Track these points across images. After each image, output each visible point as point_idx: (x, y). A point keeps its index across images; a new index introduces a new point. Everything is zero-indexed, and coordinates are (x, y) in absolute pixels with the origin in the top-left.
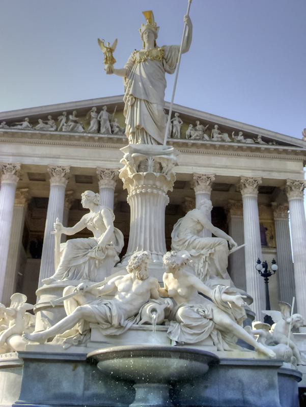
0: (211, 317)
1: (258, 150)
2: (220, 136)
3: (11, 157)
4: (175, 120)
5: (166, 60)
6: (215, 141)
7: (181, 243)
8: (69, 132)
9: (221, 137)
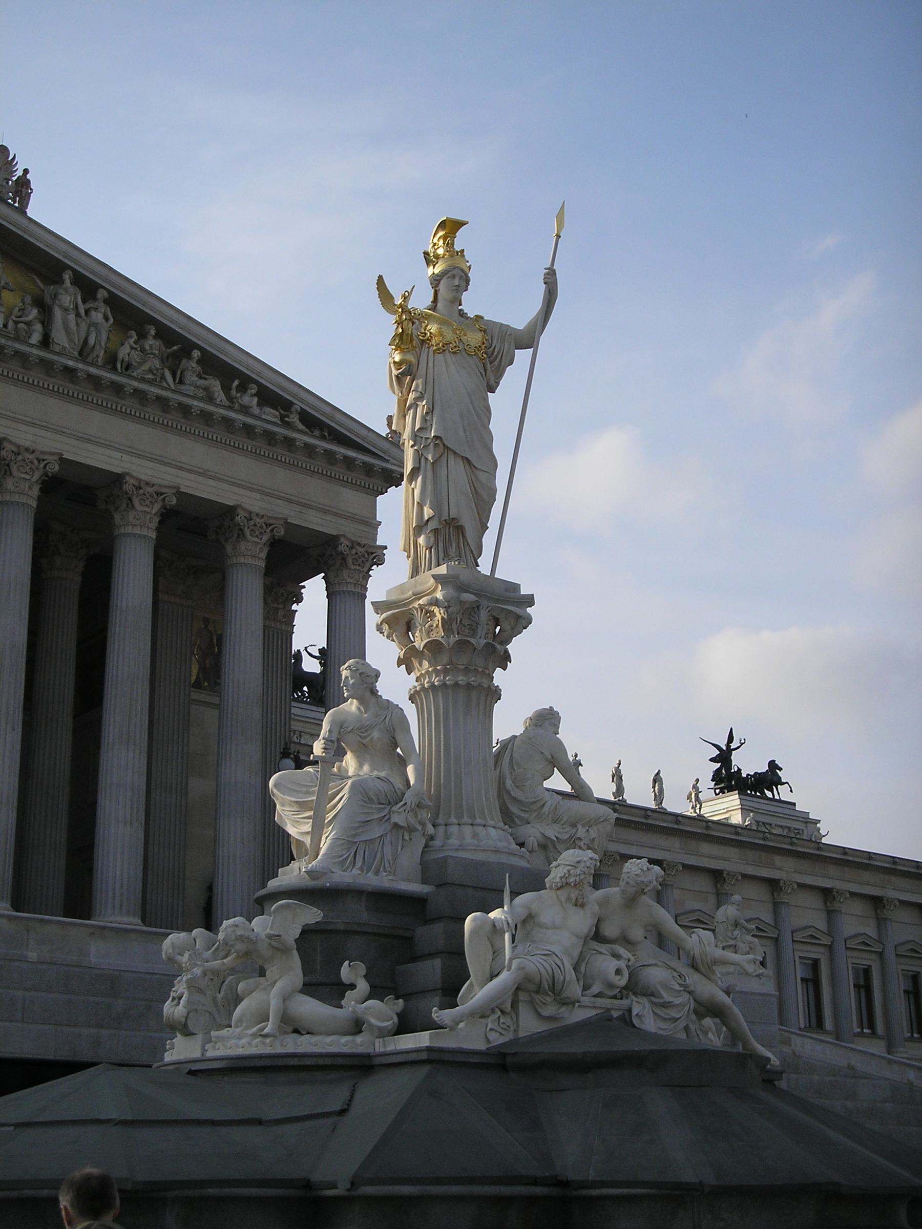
0: (692, 988)
1: (289, 443)
2: (201, 382)
4: (96, 309)
6: (194, 397)
7: (534, 807)
9: (206, 389)
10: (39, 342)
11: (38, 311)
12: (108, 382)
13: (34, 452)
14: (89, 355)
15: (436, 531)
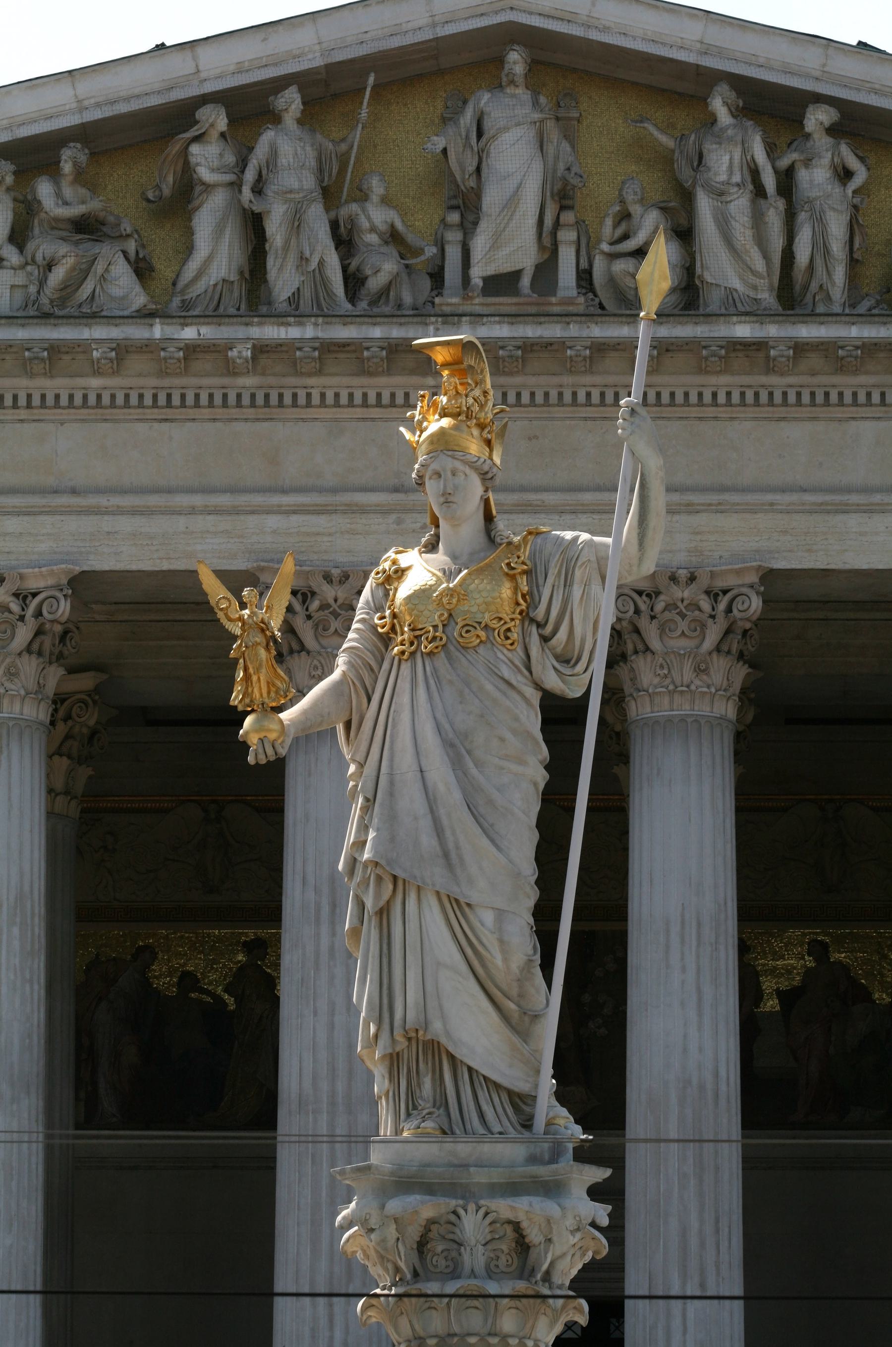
4: (808, 163)
5: (540, 626)
8: (45, 317)
10: (673, 290)
11: (663, 209)
12: (857, 348)
13: (692, 579)
14: (806, 287)
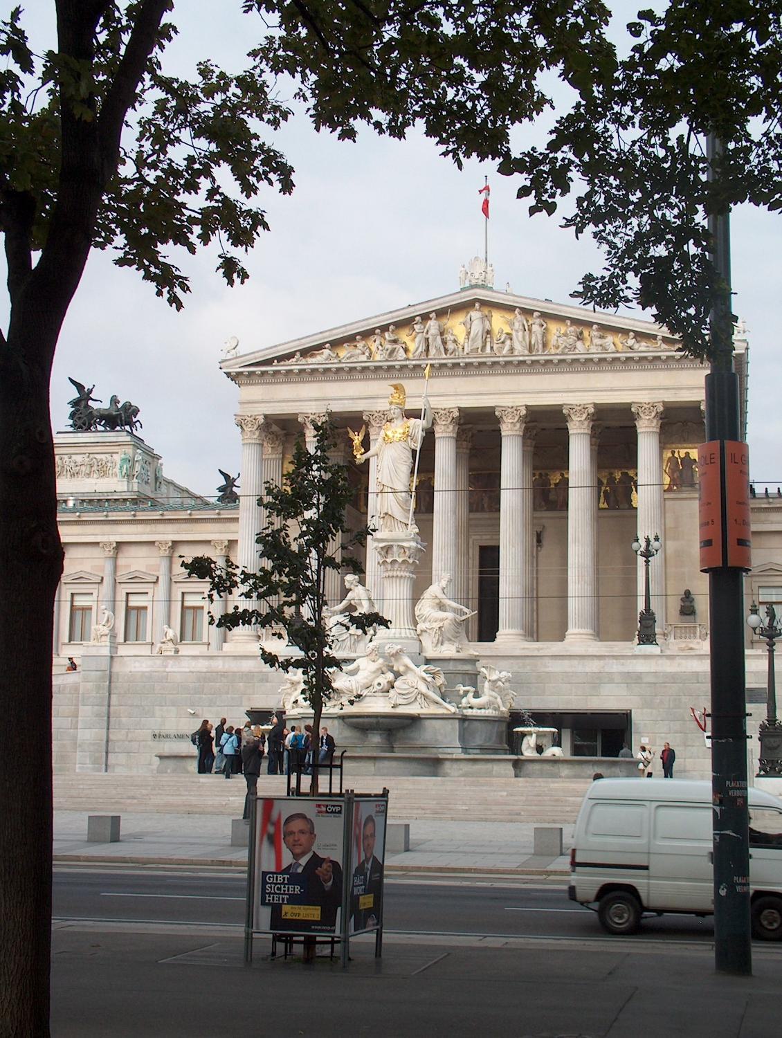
3: (314, 403)
6: (593, 353)
8: (387, 361)
9: (601, 345)
15: (383, 517)
